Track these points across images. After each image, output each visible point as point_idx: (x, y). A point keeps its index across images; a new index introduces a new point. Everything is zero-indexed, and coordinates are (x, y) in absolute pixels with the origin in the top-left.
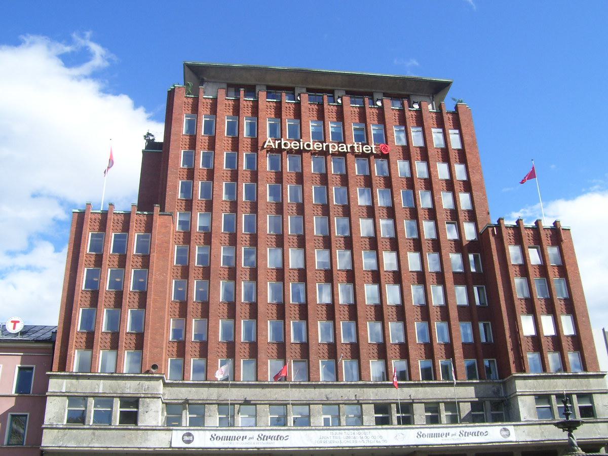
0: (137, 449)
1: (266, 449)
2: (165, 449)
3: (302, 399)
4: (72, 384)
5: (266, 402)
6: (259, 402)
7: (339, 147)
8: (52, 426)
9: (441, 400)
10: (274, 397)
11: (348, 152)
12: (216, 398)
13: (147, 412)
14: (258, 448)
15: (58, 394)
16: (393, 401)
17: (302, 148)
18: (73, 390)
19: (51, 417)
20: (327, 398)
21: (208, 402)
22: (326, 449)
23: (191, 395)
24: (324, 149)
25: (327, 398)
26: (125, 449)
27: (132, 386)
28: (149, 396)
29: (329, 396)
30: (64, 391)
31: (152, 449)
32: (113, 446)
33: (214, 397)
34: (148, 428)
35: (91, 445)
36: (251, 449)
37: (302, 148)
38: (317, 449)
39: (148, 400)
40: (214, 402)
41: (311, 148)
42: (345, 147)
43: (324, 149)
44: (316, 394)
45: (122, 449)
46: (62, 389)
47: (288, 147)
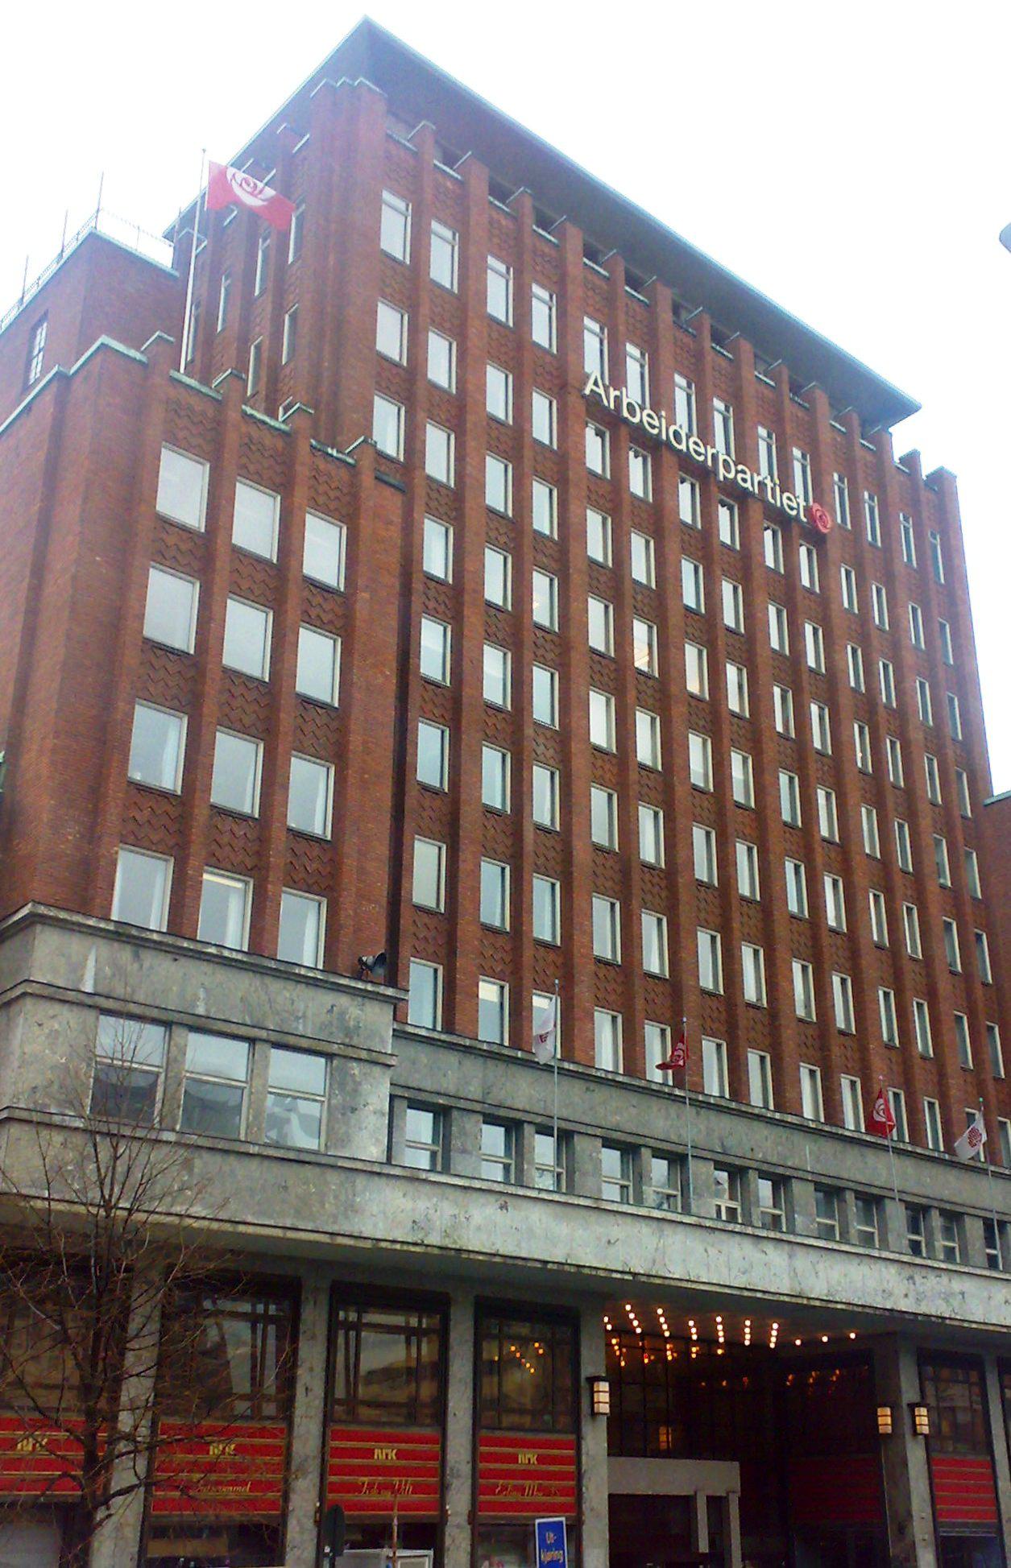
0: (325, 1239)
1: (652, 1280)
2: (405, 1248)
3: (674, 1138)
4: (119, 971)
5: (599, 1132)
6: (583, 1129)
7: (737, 472)
8: (46, 1119)
9: (935, 1204)
10: (614, 1120)
11: (752, 494)
12: (478, 1096)
13: (354, 1110)
14: (635, 1275)
15: (71, 996)
16: (851, 1185)
17: (664, 437)
18: (120, 991)
19: (39, 1081)
20: (723, 1145)
21: (462, 1104)
22: (775, 1298)
23: (417, 1076)
24: (710, 463)
25: (723, 1145)
26: (290, 1234)
27: (309, 1013)
28: (364, 1055)
29: (731, 1142)
30: (88, 987)
31: (368, 1244)
32: (250, 1219)
33: (474, 1090)
34: (359, 1165)
35: (177, 1209)
36: (619, 1276)
37: (664, 437)
38: (759, 1295)
39: (356, 1069)
40: (478, 1107)
41: (683, 447)
42: (748, 477)
43: (710, 463)
44: (700, 1131)
45: (279, 1233)
46: (81, 979)
47: (636, 420)
